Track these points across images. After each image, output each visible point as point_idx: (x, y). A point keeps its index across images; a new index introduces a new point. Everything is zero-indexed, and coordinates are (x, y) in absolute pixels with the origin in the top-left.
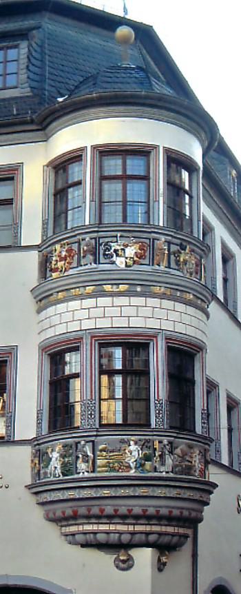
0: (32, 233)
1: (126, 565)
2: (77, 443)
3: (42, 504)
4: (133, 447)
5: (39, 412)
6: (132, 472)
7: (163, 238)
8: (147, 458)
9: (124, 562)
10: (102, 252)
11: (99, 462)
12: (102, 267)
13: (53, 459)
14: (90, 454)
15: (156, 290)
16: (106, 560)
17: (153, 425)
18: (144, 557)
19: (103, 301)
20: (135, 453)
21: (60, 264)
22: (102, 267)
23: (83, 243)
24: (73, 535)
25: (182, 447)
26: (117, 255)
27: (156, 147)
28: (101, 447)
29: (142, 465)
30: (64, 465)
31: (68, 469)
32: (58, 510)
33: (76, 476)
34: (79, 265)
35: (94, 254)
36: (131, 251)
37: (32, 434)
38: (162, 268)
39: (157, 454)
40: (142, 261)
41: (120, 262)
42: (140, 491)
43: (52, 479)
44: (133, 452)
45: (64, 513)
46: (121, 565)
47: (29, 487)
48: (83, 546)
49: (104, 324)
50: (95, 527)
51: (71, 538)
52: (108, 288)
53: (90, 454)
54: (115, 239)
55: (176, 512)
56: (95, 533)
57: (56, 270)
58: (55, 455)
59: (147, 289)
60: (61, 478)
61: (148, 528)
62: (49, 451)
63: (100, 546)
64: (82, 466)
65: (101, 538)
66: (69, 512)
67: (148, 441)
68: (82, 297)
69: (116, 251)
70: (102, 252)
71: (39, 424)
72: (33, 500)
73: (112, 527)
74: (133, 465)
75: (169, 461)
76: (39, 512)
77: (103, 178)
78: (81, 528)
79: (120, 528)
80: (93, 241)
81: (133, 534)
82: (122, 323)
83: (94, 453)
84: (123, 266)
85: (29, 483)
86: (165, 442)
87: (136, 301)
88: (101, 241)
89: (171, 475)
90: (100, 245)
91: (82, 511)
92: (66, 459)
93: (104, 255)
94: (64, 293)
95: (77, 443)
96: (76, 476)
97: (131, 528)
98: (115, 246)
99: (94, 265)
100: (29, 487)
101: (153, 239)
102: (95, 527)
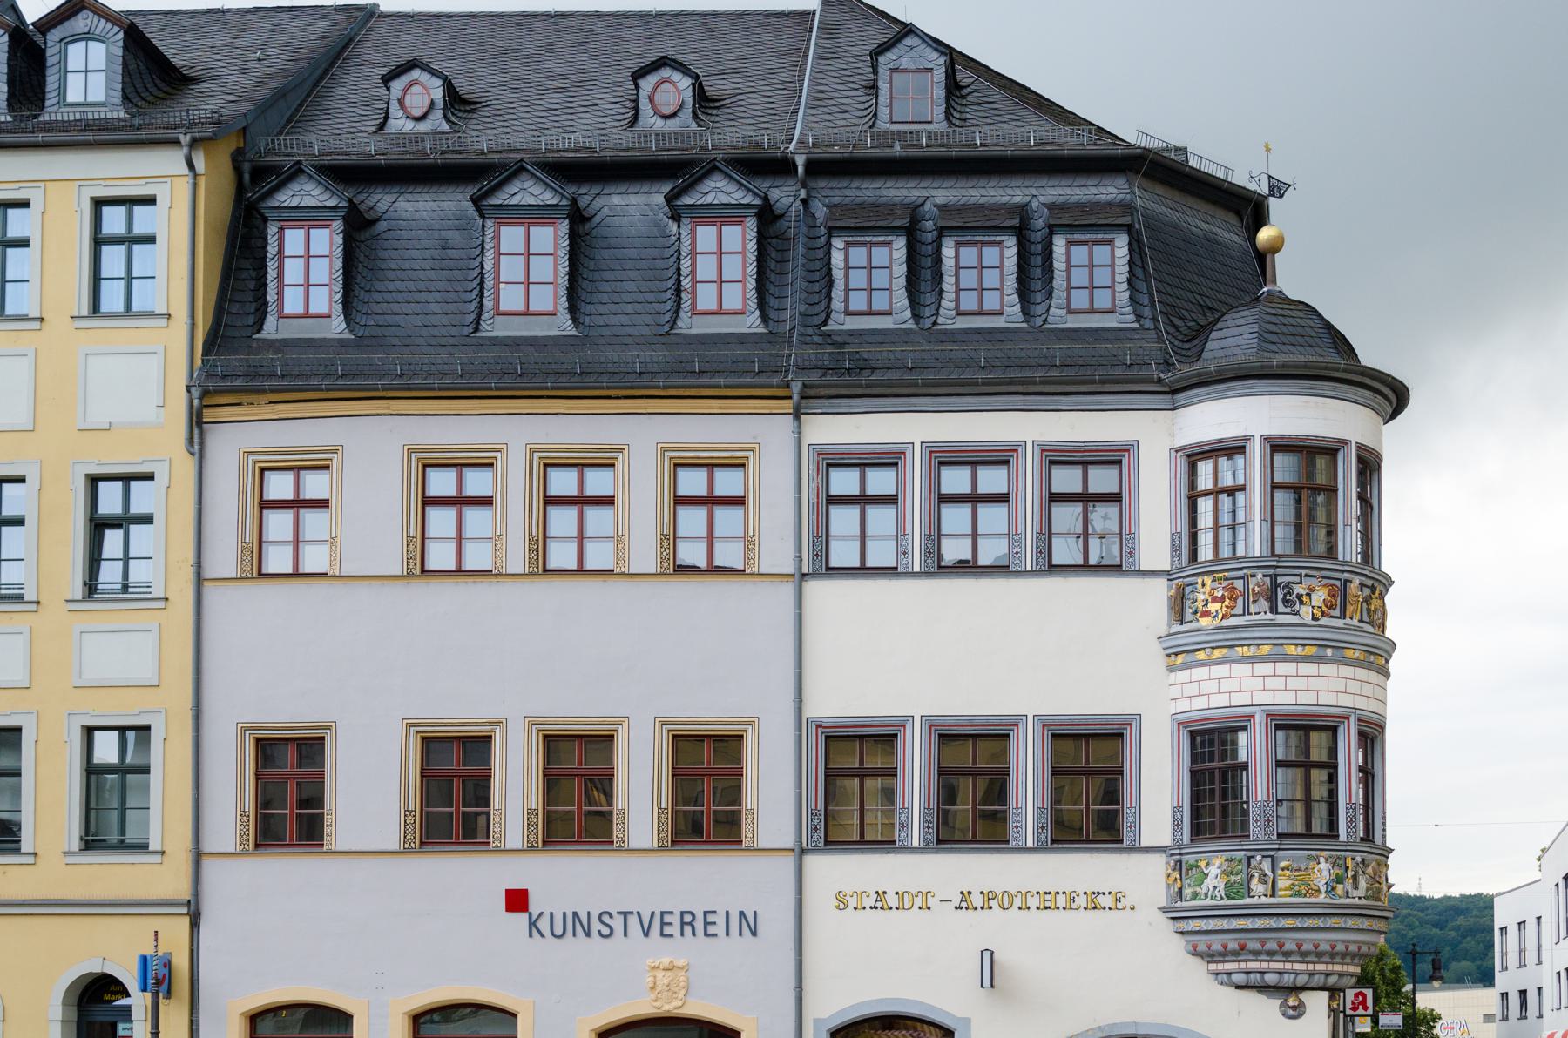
0: (1155, 549)
1: (1298, 1011)
2: (1249, 858)
3: (1182, 933)
4: (1324, 865)
5: (1178, 809)
6: (1322, 898)
7: (1357, 580)
8: (1340, 880)
9: (1294, 1008)
10: (1280, 596)
11: (1280, 884)
12: (1281, 619)
13: (1212, 876)
14: (1269, 873)
15: (1349, 654)
16: (1272, 1005)
17: (1343, 836)
18: (1317, 1003)
19: (1284, 668)
20: (1326, 873)
21: (1213, 607)
22: (1281, 619)
23: (1252, 582)
24: (1229, 974)
25: (1374, 864)
26: (1301, 603)
27: (1346, 443)
28: (1283, 864)
29: (1334, 889)
30: (1228, 886)
31: (1233, 891)
32: (1202, 943)
33: (1247, 901)
34: (1246, 612)
35: (1269, 599)
36: (1320, 597)
37: (1166, 839)
38: (1355, 622)
39: (1350, 873)
40: (1332, 613)
41: (1306, 611)
42: (1330, 922)
43: (1208, 902)
44: (1323, 871)
45: (1225, 947)
46: (1291, 1012)
47: (1164, 910)
48: (1238, 987)
49: (1288, 698)
50: (1265, 965)
51: (1224, 978)
52: (1292, 650)
53: (1269, 873)
54: (1297, 579)
55: (1340, 948)
56: (1263, 973)
57: (1206, 614)
58: (1213, 871)
59: (1338, 653)
60: (1225, 902)
61: (1330, 967)
62: (1203, 864)
63: (1263, 988)
64: (1257, 886)
65: (1271, 979)
66: (1233, 946)
67: (1339, 858)
68: (1252, 660)
69: (1299, 596)
70: (1280, 596)
71: (1177, 824)
72: (1171, 925)
73: (1288, 966)
74: (1323, 889)
75: (1363, 884)
76: (1179, 943)
77: (1275, 487)
78: (1243, 965)
79: (1297, 967)
80: (1268, 580)
81: (1312, 974)
82: (1309, 698)
83: (1273, 871)
84: (1308, 620)
85: (1163, 903)
86: (1359, 859)
87: (1327, 669)
88: (1280, 580)
89: (1364, 902)
90: (1278, 586)
91: (1253, 945)
92: (1233, 878)
93: (1286, 602)
94: (1224, 651)
95: (1249, 858)
96: (1247, 901)
97: (1310, 967)
98: (1299, 589)
99: (1269, 616)
100: (1164, 910)
101: (1346, 581)
102: (1265, 965)
